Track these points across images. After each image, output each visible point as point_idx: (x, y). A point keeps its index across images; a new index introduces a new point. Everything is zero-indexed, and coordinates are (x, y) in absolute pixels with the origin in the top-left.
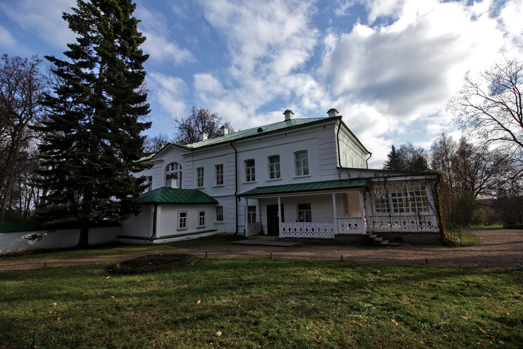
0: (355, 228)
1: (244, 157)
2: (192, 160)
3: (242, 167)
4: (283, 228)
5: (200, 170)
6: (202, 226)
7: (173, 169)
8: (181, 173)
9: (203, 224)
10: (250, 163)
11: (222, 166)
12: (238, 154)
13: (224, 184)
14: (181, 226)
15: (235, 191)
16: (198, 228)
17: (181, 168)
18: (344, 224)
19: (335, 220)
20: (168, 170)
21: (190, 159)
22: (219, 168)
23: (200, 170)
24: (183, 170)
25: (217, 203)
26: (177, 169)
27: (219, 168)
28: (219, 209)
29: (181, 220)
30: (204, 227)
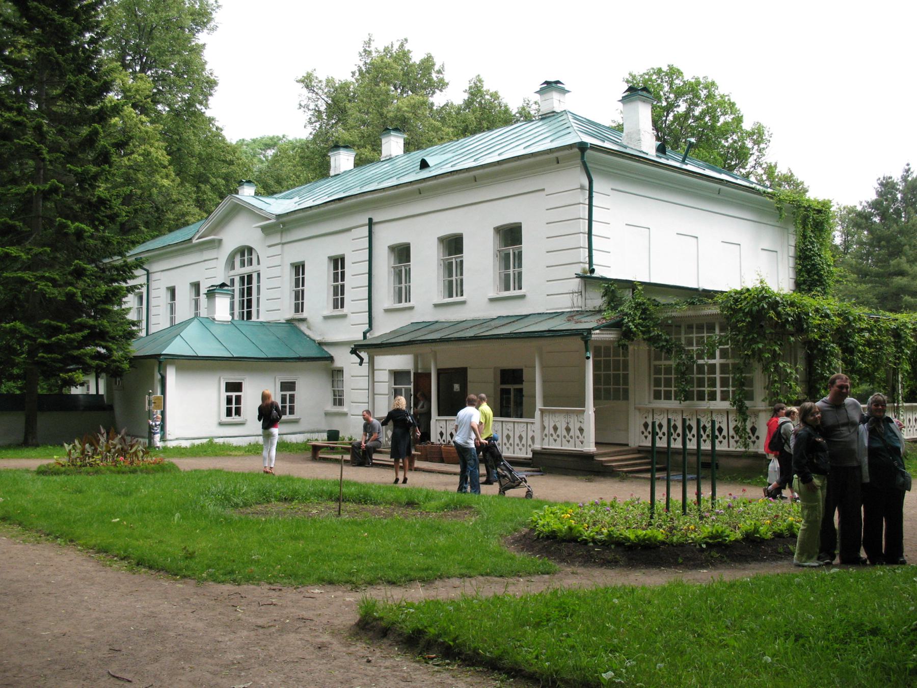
0: (565, 437)
1: (387, 236)
2: (279, 241)
3: (384, 262)
4: (439, 432)
5: (299, 268)
7: (243, 264)
8: (259, 275)
10: (402, 253)
11: (343, 259)
12: (376, 229)
13: (345, 310)
14: (229, 413)
15: (366, 327)
17: (259, 263)
18: (571, 426)
19: (538, 413)
20: (233, 268)
21: (276, 239)
22: (338, 262)
23: (299, 268)
24: (262, 268)
25: (331, 359)
27: (338, 262)
28: (336, 374)
29: (229, 400)
30: (296, 422)
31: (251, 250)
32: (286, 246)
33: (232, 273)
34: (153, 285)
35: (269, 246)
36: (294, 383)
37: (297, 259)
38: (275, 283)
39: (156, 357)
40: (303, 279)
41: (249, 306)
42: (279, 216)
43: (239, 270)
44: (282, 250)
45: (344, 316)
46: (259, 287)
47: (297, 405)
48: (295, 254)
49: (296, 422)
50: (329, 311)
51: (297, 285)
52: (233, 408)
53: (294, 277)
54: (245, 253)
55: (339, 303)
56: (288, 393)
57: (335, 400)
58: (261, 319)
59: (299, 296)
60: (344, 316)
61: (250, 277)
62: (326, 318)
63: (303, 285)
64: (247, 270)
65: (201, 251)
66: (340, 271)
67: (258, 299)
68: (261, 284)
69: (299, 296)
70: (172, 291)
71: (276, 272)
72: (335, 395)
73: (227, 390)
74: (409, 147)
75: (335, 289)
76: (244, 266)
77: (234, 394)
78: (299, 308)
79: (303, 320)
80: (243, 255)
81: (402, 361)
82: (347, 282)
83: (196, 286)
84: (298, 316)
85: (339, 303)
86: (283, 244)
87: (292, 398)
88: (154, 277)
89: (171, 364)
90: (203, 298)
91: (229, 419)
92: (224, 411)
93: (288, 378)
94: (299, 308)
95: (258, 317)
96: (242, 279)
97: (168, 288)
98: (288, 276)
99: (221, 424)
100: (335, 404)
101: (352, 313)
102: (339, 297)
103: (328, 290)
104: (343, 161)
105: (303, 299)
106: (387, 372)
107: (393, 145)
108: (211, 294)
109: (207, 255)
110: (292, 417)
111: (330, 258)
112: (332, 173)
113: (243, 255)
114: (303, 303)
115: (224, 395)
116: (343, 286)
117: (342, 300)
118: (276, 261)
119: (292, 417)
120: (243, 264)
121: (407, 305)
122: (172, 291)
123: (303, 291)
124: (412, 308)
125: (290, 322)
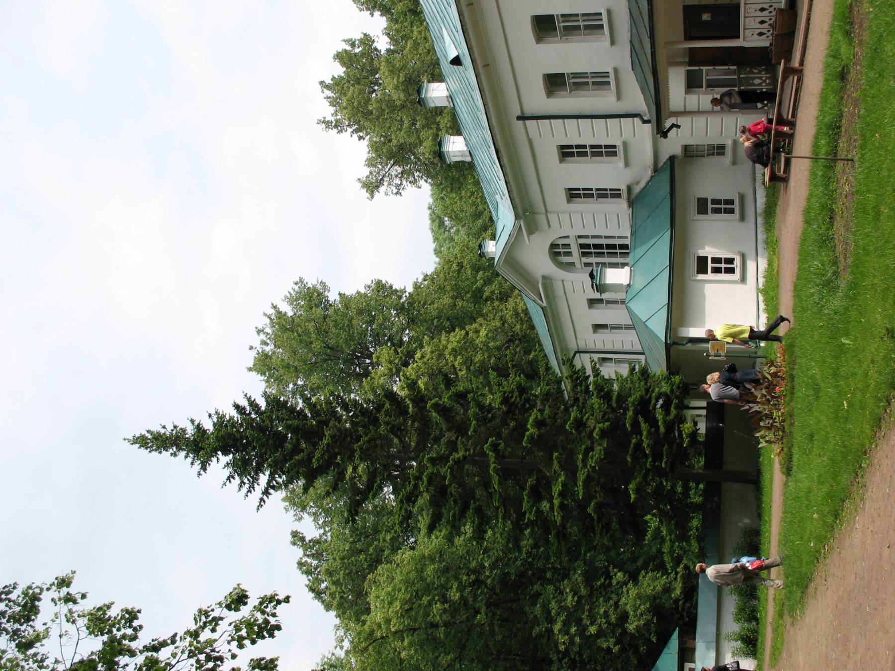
2: (543, 217)
3: (565, 102)
5: (573, 194)
6: (736, 206)
7: (569, 254)
8: (580, 237)
9: (731, 202)
11: (563, 147)
12: (528, 112)
13: (618, 143)
14: (731, 271)
15: (637, 120)
16: (742, 218)
17: (568, 237)
20: (573, 264)
21: (542, 218)
22: (566, 152)
23: (573, 194)
24: (573, 233)
25: (672, 159)
26: (567, 246)
27: (566, 152)
28: (690, 153)
29: (717, 270)
30: (742, 197)
31: (553, 246)
32: (549, 208)
33: (578, 265)
34: (591, 346)
35: (549, 226)
36: (699, 199)
37: (563, 196)
38: (588, 218)
39: (668, 347)
40: (584, 189)
41: (613, 246)
42: (517, 217)
43: (576, 256)
44: (551, 212)
45: (625, 144)
46: (593, 237)
47: (723, 196)
48: (557, 199)
49: (742, 197)
50: (619, 162)
51: (591, 196)
52: (725, 266)
53: (582, 199)
54: (557, 251)
55: (610, 151)
56: (710, 206)
57: (719, 154)
58: (628, 234)
59: (603, 194)
60: (625, 144)
61: (582, 246)
62: (627, 164)
63: (592, 189)
64: (574, 249)
65: (554, 296)
66: (575, 150)
67: (606, 237)
68: (590, 234)
69: (603, 194)
70: (597, 327)
71: (576, 218)
72: (713, 154)
73: (705, 272)
74: (438, 77)
75: (594, 154)
76: (571, 252)
77: (710, 265)
78: (615, 194)
79: (629, 189)
80: (559, 254)
81: (676, 80)
82: (588, 142)
83: (592, 302)
84: (624, 194)
85: (610, 151)
86: (547, 212)
87: (715, 202)
88: (582, 346)
89: (676, 331)
90: (605, 296)
91: (738, 271)
92: (729, 277)
93: (693, 207)
94: (615, 194)
95: (627, 237)
96: (584, 254)
97: (594, 332)
98: (580, 206)
99: (743, 279)
100: (723, 154)
101: (621, 136)
102: (603, 150)
103: (598, 162)
104: (455, 146)
105: (606, 190)
106: (687, 96)
107: (436, 93)
108: (601, 288)
109: (559, 291)
110: (737, 202)
111: (561, 161)
112: (468, 159)
113: (559, 254)
114: (610, 190)
115: (710, 276)
116: (592, 147)
117: (606, 147)
118: (565, 218)
119: (737, 202)
120: (569, 254)
121: (612, 75)
122: (597, 327)
123: (597, 190)
124: (616, 70)
125: (631, 204)
